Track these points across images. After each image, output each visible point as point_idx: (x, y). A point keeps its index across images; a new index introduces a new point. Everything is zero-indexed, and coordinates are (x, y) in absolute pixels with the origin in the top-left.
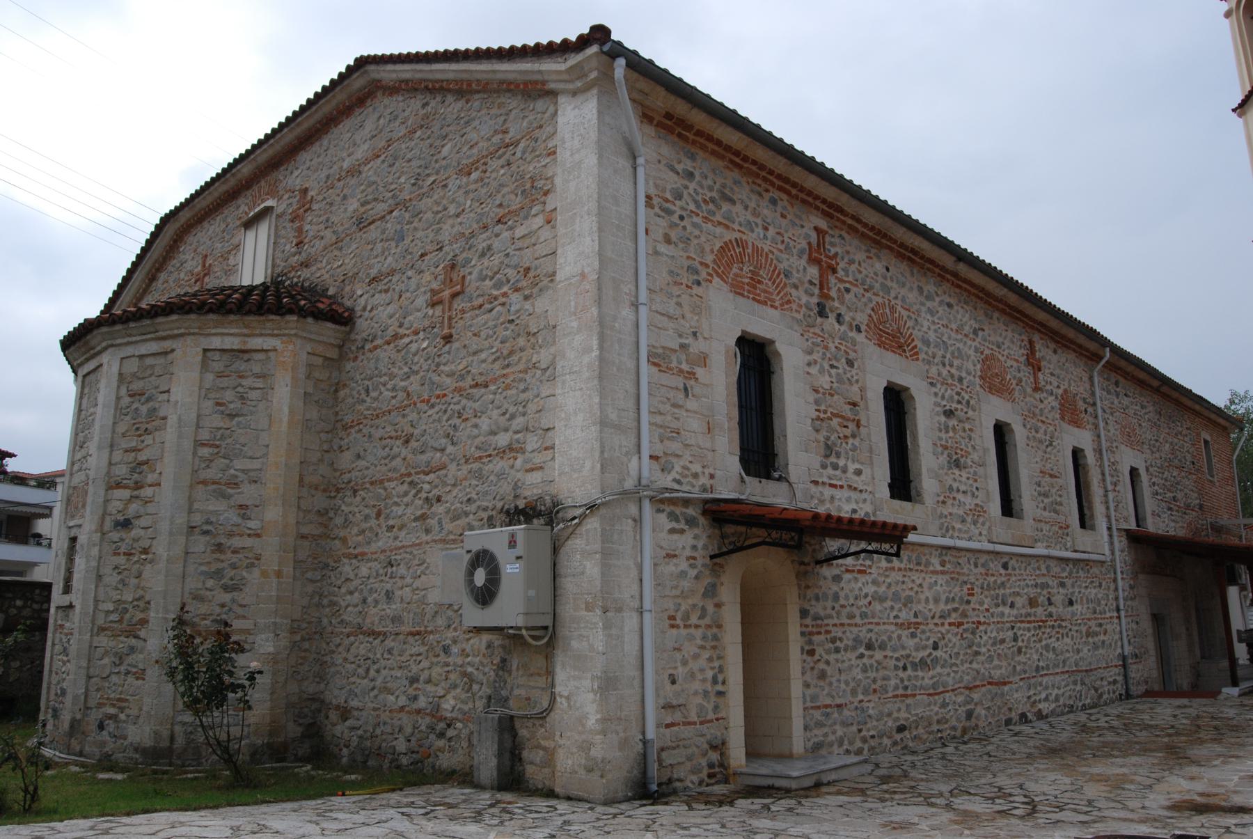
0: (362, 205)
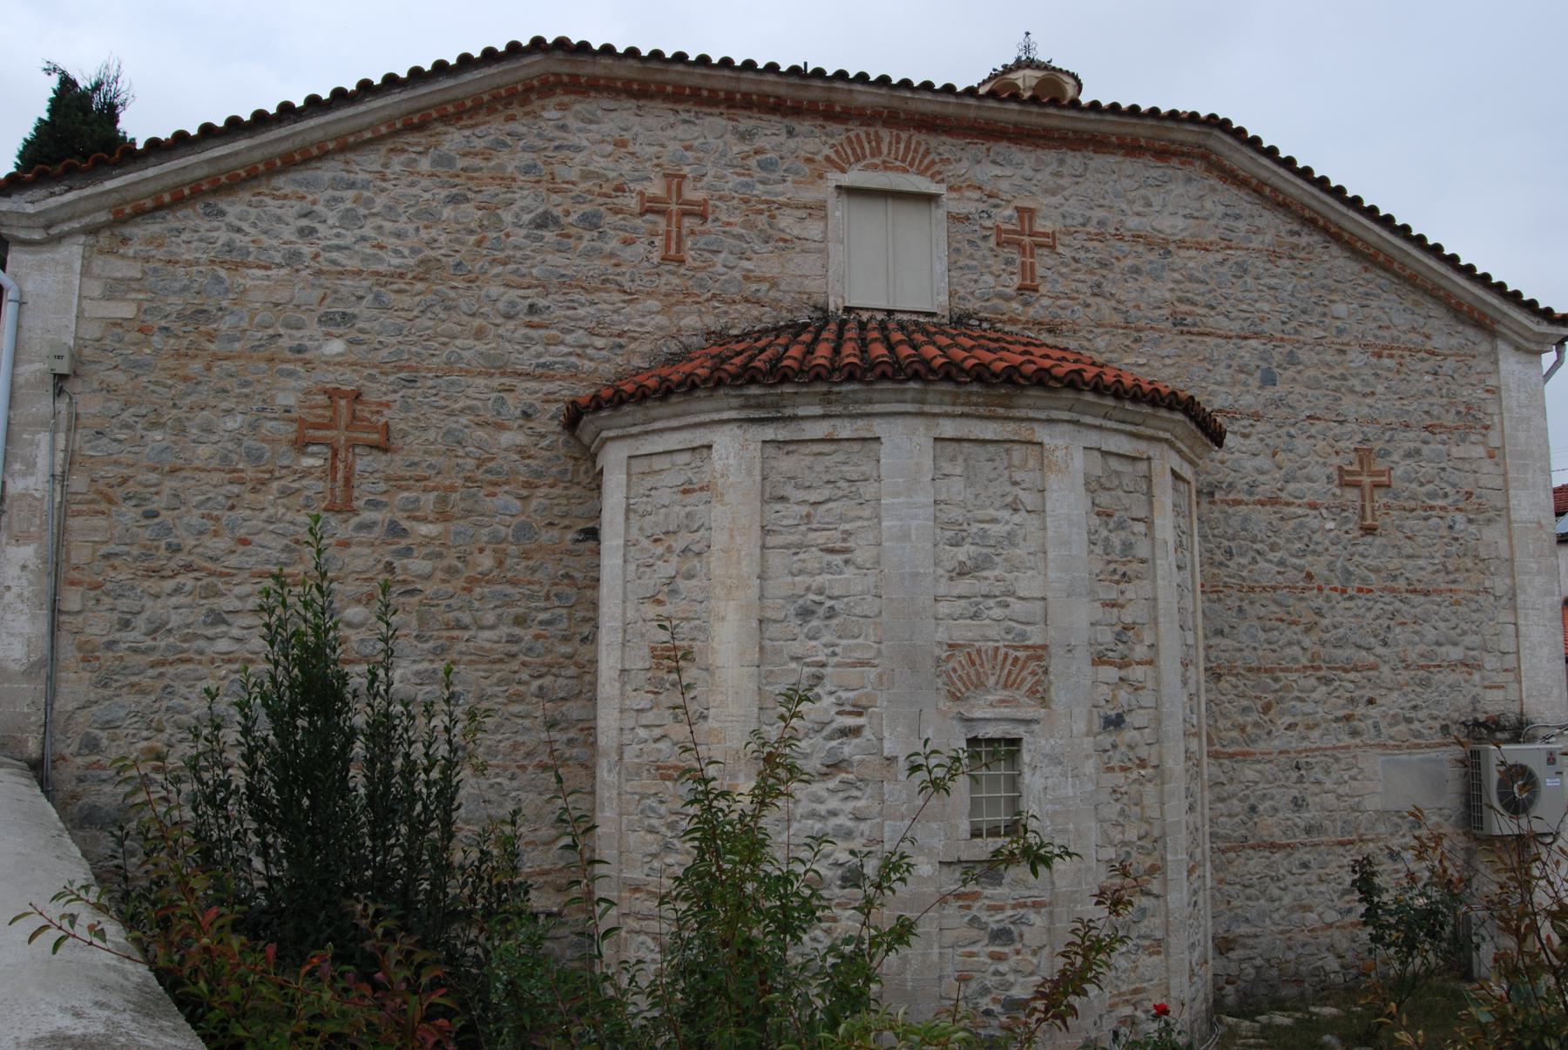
0: (1180, 300)
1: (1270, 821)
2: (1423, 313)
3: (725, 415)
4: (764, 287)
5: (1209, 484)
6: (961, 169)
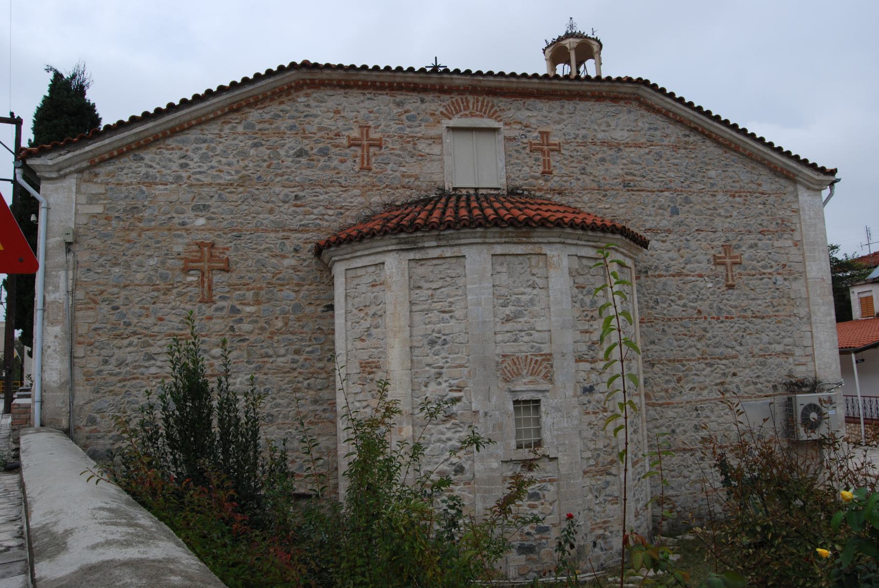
0: (627, 174)
1: (682, 437)
2: (757, 173)
3: (390, 248)
4: (412, 180)
5: (645, 267)
6: (510, 114)
